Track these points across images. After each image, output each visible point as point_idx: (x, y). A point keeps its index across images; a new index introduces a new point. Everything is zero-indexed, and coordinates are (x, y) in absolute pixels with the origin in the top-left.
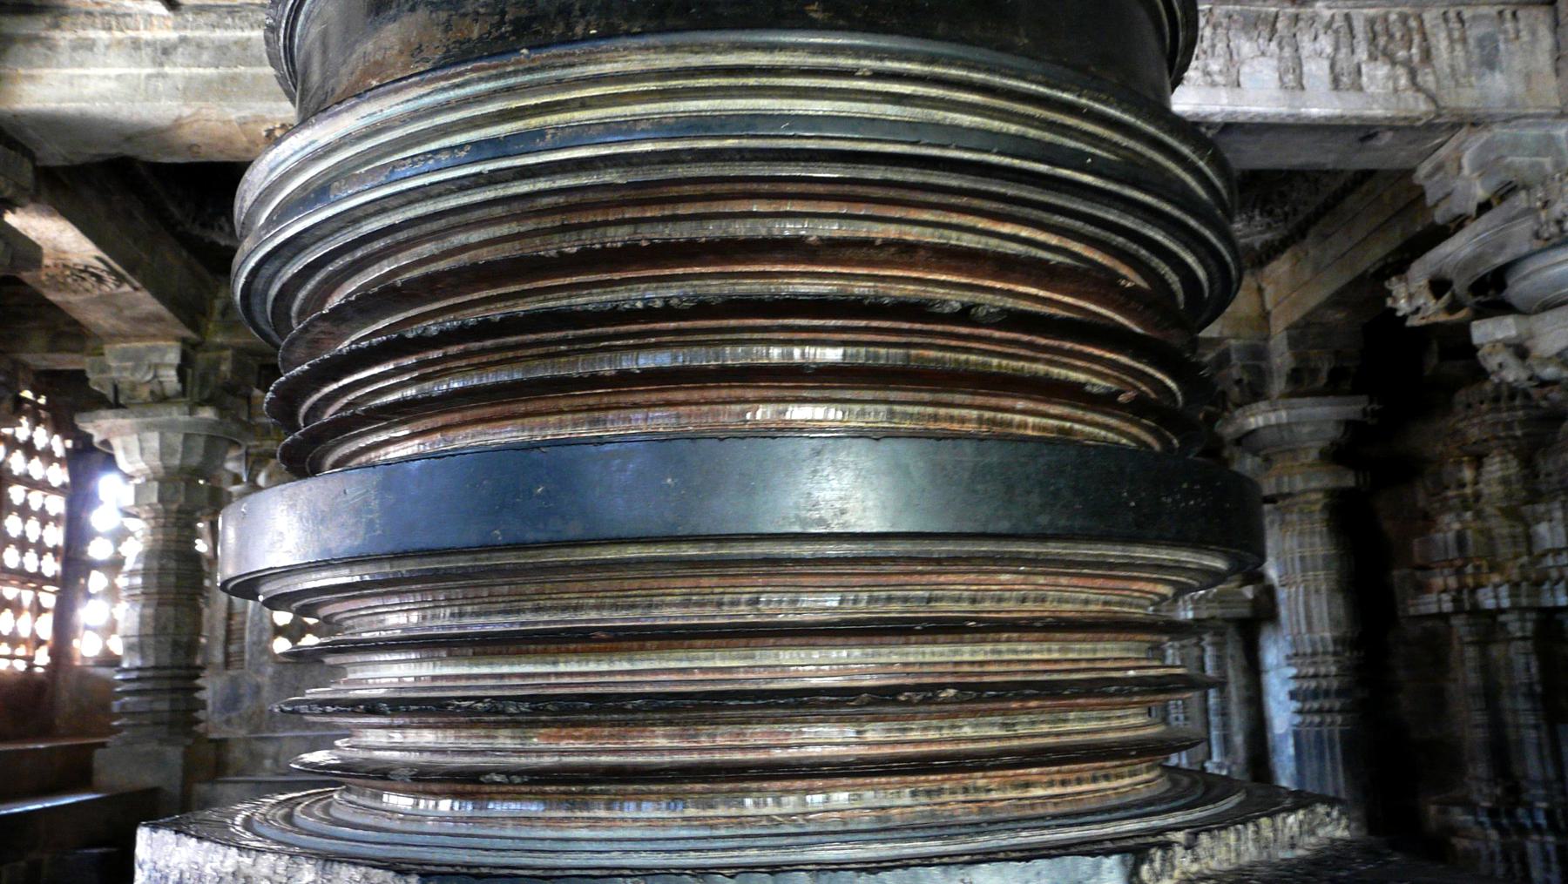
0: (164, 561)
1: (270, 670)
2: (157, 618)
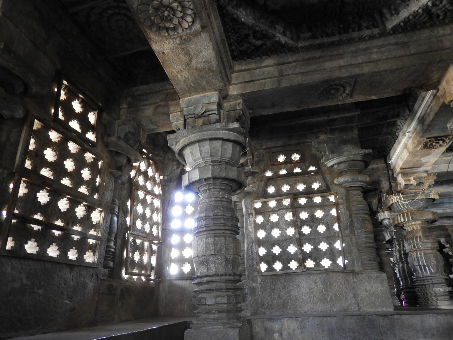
0: (216, 211)
1: (259, 280)
2: (215, 244)
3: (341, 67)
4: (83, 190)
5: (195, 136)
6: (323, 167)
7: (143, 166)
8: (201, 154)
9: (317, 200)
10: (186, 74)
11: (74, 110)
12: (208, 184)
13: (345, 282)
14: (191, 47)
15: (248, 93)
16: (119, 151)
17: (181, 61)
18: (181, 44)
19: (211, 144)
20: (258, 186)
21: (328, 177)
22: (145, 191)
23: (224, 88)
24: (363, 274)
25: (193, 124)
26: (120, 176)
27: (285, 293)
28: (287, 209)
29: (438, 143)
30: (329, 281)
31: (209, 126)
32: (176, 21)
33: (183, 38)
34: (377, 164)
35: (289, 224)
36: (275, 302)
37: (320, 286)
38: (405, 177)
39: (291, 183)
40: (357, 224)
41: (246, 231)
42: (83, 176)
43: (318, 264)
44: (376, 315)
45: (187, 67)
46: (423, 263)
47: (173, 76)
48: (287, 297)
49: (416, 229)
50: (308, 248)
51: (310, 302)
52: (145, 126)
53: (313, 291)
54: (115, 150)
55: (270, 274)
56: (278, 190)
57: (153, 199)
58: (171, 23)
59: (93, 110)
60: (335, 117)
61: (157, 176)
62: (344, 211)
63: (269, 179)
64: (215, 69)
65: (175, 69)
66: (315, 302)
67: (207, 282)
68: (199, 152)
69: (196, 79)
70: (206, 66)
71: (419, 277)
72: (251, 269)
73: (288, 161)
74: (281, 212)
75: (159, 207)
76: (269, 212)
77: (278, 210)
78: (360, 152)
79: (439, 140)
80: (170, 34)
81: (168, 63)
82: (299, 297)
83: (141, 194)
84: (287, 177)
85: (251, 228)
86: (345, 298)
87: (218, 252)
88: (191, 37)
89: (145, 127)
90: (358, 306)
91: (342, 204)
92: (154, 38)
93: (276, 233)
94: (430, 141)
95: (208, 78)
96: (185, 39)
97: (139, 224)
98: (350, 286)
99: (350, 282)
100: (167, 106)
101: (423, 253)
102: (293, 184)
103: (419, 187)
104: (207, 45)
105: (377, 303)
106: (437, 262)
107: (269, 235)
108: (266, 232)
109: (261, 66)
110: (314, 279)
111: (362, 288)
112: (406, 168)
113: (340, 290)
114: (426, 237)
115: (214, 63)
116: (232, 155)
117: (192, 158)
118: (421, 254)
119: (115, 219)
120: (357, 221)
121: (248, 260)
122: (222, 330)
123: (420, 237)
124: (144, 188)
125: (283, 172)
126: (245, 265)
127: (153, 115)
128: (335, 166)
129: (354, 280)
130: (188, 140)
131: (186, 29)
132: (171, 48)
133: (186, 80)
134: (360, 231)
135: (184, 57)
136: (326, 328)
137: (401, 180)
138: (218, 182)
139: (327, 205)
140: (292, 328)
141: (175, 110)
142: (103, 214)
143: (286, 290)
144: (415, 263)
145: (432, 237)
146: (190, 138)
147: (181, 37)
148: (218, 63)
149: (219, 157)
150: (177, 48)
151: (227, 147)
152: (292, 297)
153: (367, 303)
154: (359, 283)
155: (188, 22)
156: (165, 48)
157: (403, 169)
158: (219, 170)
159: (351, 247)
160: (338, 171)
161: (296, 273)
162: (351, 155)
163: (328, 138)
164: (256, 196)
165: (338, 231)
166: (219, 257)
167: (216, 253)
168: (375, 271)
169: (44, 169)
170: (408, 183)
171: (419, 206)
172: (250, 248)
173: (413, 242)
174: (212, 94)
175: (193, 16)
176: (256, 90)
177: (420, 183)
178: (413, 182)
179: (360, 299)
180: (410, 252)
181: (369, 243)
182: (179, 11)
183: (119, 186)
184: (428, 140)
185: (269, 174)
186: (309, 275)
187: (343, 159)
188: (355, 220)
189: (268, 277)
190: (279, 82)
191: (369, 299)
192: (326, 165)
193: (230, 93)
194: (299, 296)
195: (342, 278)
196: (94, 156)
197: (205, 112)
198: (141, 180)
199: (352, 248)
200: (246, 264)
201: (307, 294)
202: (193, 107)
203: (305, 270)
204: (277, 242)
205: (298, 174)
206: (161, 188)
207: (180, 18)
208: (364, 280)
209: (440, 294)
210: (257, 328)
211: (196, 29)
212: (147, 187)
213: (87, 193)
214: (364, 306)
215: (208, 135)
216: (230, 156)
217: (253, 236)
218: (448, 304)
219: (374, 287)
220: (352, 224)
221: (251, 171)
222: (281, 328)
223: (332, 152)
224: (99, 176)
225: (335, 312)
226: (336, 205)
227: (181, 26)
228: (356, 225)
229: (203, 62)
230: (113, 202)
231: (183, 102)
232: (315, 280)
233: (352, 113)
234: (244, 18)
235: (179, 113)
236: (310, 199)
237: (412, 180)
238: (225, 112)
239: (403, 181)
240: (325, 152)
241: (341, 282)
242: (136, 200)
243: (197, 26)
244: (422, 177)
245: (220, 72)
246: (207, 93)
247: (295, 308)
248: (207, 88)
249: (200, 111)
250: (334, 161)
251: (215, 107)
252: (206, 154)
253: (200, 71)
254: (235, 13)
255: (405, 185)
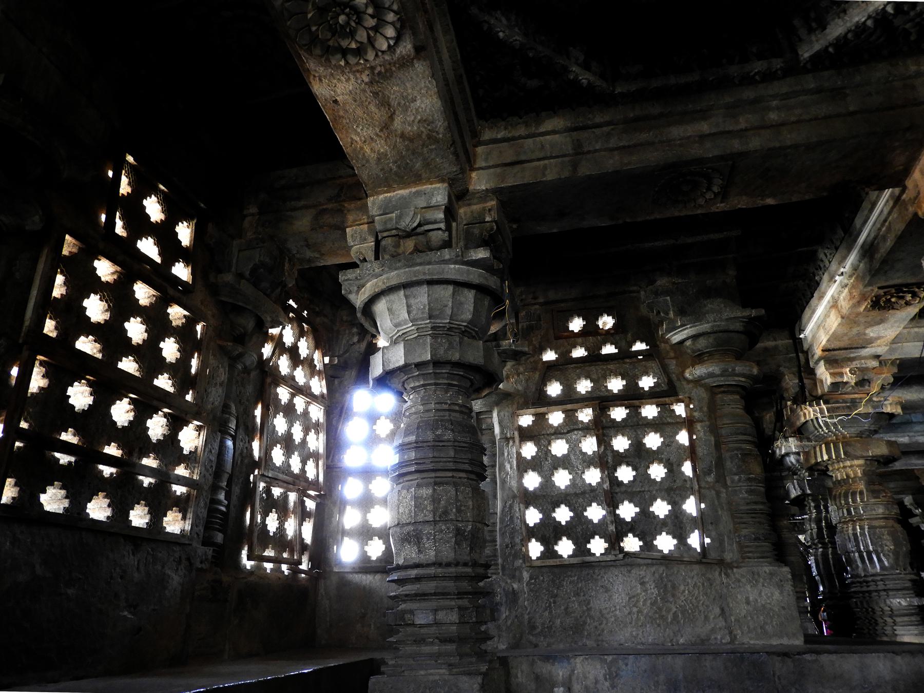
0: (439, 432)
1: (526, 575)
2: (435, 500)
3: (703, 137)
4: (164, 382)
5: (398, 275)
6: (663, 345)
7: (288, 335)
8: (409, 312)
9: (650, 411)
10: (381, 146)
11: (148, 217)
12: (423, 374)
13: (703, 584)
14: (394, 91)
15: (511, 186)
16: (240, 304)
17: (372, 118)
18: (371, 82)
19: (431, 292)
20: (527, 381)
21: (673, 365)
22: (291, 387)
23: (460, 176)
24: (741, 567)
25: (393, 249)
26: (241, 356)
27: (580, 604)
28: (586, 429)
29: (902, 298)
30: (670, 581)
31: (427, 255)
32: (362, 36)
33: (376, 72)
34: (775, 340)
35: (589, 461)
36: (558, 622)
37: (653, 590)
38: (833, 367)
39: (594, 377)
40: (732, 462)
41: (500, 473)
42: (164, 354)
43: (648, 545)
44: (767, 653)
45: (384, 130)
46: (866, 546)
47: (355, 150)
48: (584, 612)
49: (852, 476)
50: (627, 511)
51: (631, 623)
52: (295, 252)
53: (638, 601)
54: (230, 301)
55: (548, 564)
56: (569, 389)
57: (308, 403)
58: (352, 39)
59: (187, 218)
60: (690, 240)
61: (317, 356)
62: (705, 435)
63: (550, 364)
64: (441, 136)
65: (358, 134)
66: (640, 624)
67: (418, 579)
68: (406, 308)
69: (402, 157)
70: (423, 130)
71: (858, 576)
72: (510, 553)
73: (591, 332)
74: (574, 436)
75: (321, 420)
76: (548, 435)
77: (568, 432)
78: (739, 314)
79: (905, 292)
80: (350, 62)
81: (344, 121)
82: (608, 613)
83: (283, 393)
84: (588, 364)
85: (510, 468)
86: (703, 617)
87: (440, 517)
88: (394, 69)
89: (294, 255)
90: (731, 633)
91: (701, 421)
92: (315, 71)
93: (562, 479)
94: (885, 293)
95: (427, 155)
96: (380, 73)
97: (278, 456)
98: (713, 592)
99: (715, 584)
100: (341, 211)
101: (866, 527)
102: (599, 378)
103: (861, 389)
104: (425, 86)
105: (769, 628)
106: (895, 545)
107: (548, 482)
108: (542, 477)
109: (537, 131)
110: (640, 575)
111: (739, 597)
112: (834, 350)
113: (694, 601)
114: (874, 493)
115: (440, 124)
116: (473, 315)
117: (391, 321)
118: (862, 528)
119: (230, 443)
120: (731, 458)
121: (503, 534)
122: (446, 677)
123: (861, 493)
124: (289, 381)
125: (579, 352)
126: (496, 545)
127: (312, 230)
128: (688, 343)
129: (722, 580)
130: (384, 283)
131: (383, 52)
132: (350, 92)
133: (381, 157)
134: (737, 478)
135: (377, 111)
136: (662, 678)
137: (824, 374)
138: (444, 371)
139: (669, 424)
140: (591, 677)
141: (356, 221)
142: (203, 434)
143: (582, 598)
144: (851, 546)
145: (886, 493)
146: (388, 279)
147: (372, 68)
148: (449, 124)
149: (446, 319)
150: (364, 91)
151: (463, 299)
152: (592, 613)
153: (748, 627)
154: (733, 586)
155: (387, 38)
156: (339, 91)
157: (829, 350)
158: (446, 346)
159: (717, 512)
160: (694, 352)
161: (603, 564)
162: (721, 320)
163: (674, 283)
164: (521, 401)
165: (691, 476)
166: (443, 527)
167: (438, 519)
168: (766, 562)
169: (82, 338)
170: (839, 380)
171: (861, 429)
172: (508, 510)
173: (847, 503)
174: (435, 188)
175: (398, 26)
176: (526, 181)
177: (864, 380)
178: (848, 377)
179: (735, 620)
180: (840, 523)
181: (756, 503)
182: (370, 15)
183: (238, 375)
184: (881, 292)
185: (550, 356)
186: (629, 568)
187: (705, 327)
188: (727, 455)
189: (544, 570)
190: (575, 166)
191: (752, 618)
192: (668, 339)
193: (471, 188)
194: (608, 610)
195: (698, 575)
196: (186, 313)
197: (420, 225)
198: (284, 365)
199: (720, 513)
200: (498, 543)
201: (625, 607)
202: (394, 215)
203: (621, 556)
204: (562, 498)
205: (610, 357)
206: (324, 381)
207: (371, 28)
208: (744, 580)
209: (902, 612)
210: (519, 675)
211: (404, 52)
212: (297, 380)
213: (171, 390)
214: (742, 633)
215: (424, 274)
216: (470, 317)
217: (514, 484)
218: (916, 632)
219: (763, 594)
220: (720, 463)
221: (513, 350)
222: (570, 677)
223: (682, 312)
224: (196, 355)
225: (683, 644)
226: (689, 423)
227: (373, 47)
228: (728, 464)
229: (417, 121)
230: (226, 408)
231: (374, 203)
232: (643, 578)
233: (725, 233)
234: (504, 32)
235: (366, 226)
236: (634, 411)
237: (846, 374)
238: (461, 226)
239: (828, 377)
240: (667, 314)
241: (696, 584)
242: (272, 406)
243: (406, 48)
244: (867, 369)
245: (451, 143)
246: (425, 187)
247: (599, 635)
248: (424, 175)
249: (409, 222)
250: (686, 332)
251: (442, 216)
252: (420, 312)
253: (411, 140)
254: (485, 21)
255: (832, 384)
